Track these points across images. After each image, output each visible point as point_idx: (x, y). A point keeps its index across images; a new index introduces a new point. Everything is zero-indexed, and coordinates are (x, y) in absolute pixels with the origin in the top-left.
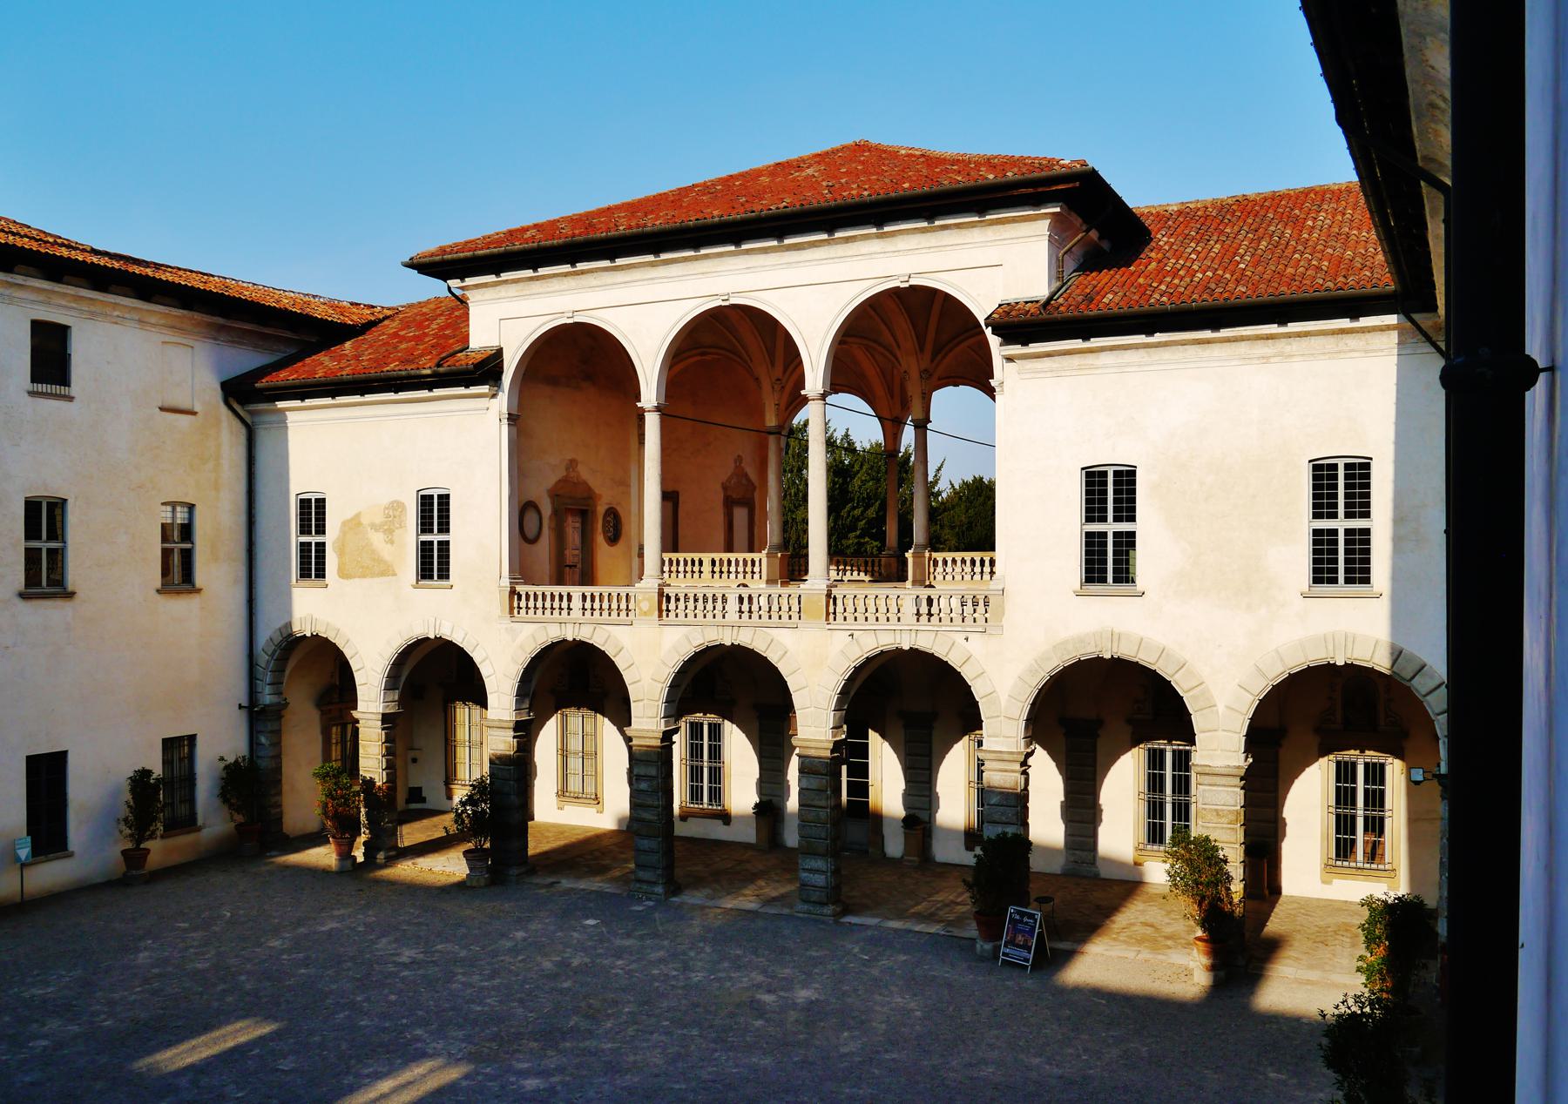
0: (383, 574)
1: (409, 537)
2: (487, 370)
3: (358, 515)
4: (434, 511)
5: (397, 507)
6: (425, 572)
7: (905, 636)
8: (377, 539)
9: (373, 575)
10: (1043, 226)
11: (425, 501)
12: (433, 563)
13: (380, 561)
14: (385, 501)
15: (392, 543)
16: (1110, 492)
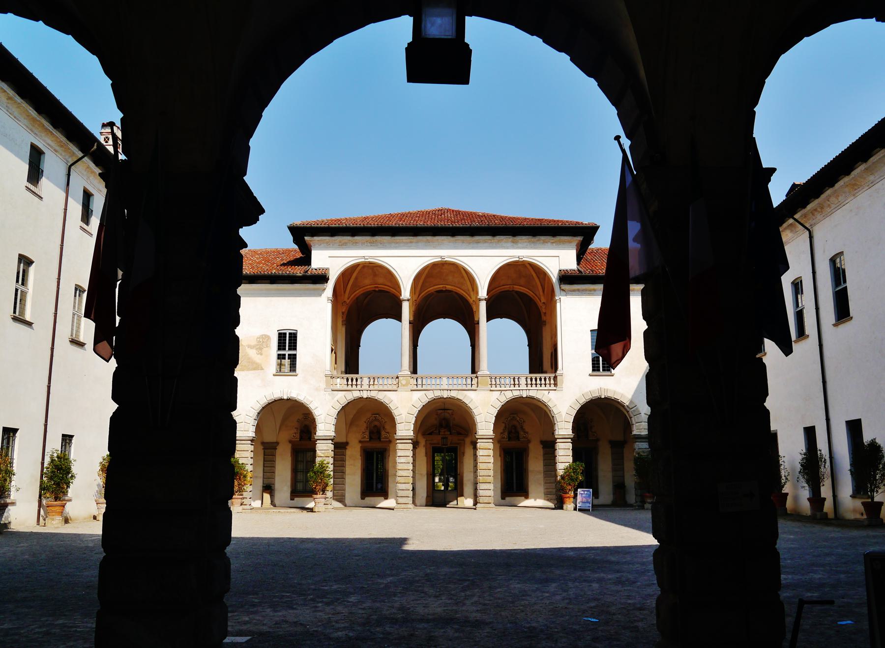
0: (254, 369)
2: (321, 278)
4: (288, 341)
5: (266, 338)
9: (249, 369)
10: (574, 244)
11: (282, 336)
15: (261, 354)
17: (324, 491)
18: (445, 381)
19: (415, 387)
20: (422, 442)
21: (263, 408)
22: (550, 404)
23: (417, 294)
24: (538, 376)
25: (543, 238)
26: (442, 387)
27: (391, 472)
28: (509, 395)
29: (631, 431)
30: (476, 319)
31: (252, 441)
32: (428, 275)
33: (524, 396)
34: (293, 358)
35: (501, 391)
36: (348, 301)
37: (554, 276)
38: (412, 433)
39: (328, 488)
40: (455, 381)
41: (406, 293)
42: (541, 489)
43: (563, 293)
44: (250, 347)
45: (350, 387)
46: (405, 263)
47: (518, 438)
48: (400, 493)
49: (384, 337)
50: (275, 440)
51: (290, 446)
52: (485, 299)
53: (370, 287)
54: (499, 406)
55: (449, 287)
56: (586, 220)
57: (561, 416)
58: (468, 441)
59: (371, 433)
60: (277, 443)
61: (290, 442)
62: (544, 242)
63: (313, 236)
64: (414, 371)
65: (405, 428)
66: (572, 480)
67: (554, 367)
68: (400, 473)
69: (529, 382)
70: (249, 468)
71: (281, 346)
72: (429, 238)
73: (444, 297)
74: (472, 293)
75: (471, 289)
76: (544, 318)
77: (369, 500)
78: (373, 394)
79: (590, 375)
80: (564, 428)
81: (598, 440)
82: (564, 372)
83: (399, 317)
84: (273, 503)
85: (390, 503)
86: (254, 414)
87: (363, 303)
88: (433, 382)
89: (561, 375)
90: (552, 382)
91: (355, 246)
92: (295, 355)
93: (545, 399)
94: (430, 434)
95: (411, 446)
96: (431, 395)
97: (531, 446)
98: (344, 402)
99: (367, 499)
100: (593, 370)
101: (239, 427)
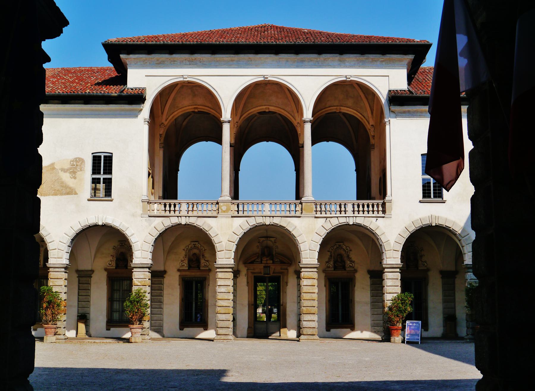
0: (68, 194)
2: (137, 98)
3: (53, 164)
4: (103, 164)
5: (78, 162)
7: (351, 219)
8: (66, 177)
9: (62, 194)
11: (96, 159)
13: (67, 187)
14: (72, 157)
15: (75, 178)
17: (140, 321)
18: (267, 207)
19: (236, 214)
20: (244, 271)
21: (77, 234)
22: (378, 232)
23: (239, 115)
25: (371, 56)
26: (265, 214)
27: (210, 302)
28: (335, 222)
29: (463, 262)
30: (301, 142)
31: (66, 268)
33: (351, 223)
34: (108, 183)
35: (327, 218)
36: (166, 123)
37: (383, 97)
38: (232, 262)
39: (144, 318)
40: (278, 208)
41: (226, 114)
42: (368, 321)
43: (392, 114)
44: (64, 170)
45: (167, 213)
46: (226, 82)
47: (344, 268)
48: (220, 324)
49: (204, 162)
50: (90, 268)
51: (105, 273)
52: (310, 121)
53: (190, 109)
54: (324, 233)
55: (272, 109)
56: (418, 38)
57: (390, 244)
58: (291, 270)
59: (190, 261)
60: (92, 271)
61: (106, 270)
62: (373, 61)
63: (128, 53)
64: (235, 195)
65: (225, 255)
66: (401, 311)
67: (383, 193)
68: (220, 303)
69: (356, 209)
70: (63, 296)
71: (96, 170)
72: (251, 56)
73: (266, 120)
74: (296, 115)
75: (295, 111)
76: (372, 141)
77: (188, 331)
78: (192, 221)
79: (420, 202)
80: (392, 257)
81: (428, 270)
82: (394, 198)
83: (219, 140)
84: (88, 333)
85: (210, 334)
86: (67, 240)
87: (181, 126)
88: (255, 208)
89: (390, 201)
90: (380, 208)
91: (173, 65)
92: (111, 179)
93: (372, 227)
94: (252, 262)
95: (231, 275)
96: (253, 222)
97: (358, 276)
98: (161, 229)
99: (185, 329)
100: (424, 197)
101: (51, 254)
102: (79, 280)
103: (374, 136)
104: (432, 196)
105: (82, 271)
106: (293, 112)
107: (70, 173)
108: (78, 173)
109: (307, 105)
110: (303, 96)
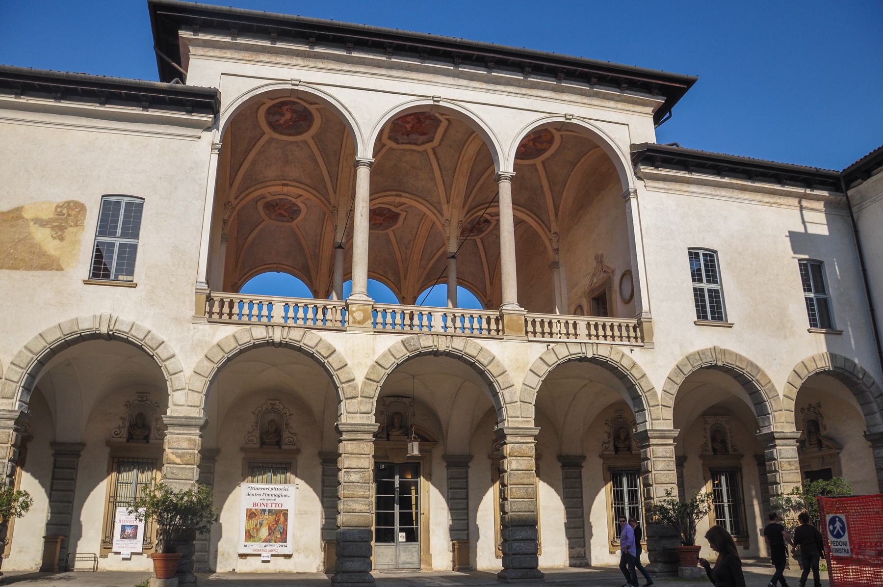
0: (43, 268)
1: (87, 237)
3: (19, 209)
4: (121, 218)
6: (100, 271)
8: (42, 236)
9: (30, 268)
12: (110, 265)
15: (62, 239)
16: (704, 264)
24: (601, 320)
28: (563, 352)
32: (412, 127)
44: (41, 223)
51: (107, 450)
57: (655, 394)
74: (445, 207)
75: (443, 199)
89: (650, 321)
100: (699, 317)
102: (55, 461)
103: (558, 249)
104: (709, 317)
105: (63, 444)
106: (439, 203)
107: (53, 228)
108: (70, 229)
109: (506, 151)
110: (499, 137)
